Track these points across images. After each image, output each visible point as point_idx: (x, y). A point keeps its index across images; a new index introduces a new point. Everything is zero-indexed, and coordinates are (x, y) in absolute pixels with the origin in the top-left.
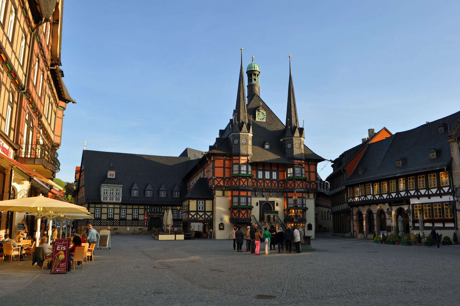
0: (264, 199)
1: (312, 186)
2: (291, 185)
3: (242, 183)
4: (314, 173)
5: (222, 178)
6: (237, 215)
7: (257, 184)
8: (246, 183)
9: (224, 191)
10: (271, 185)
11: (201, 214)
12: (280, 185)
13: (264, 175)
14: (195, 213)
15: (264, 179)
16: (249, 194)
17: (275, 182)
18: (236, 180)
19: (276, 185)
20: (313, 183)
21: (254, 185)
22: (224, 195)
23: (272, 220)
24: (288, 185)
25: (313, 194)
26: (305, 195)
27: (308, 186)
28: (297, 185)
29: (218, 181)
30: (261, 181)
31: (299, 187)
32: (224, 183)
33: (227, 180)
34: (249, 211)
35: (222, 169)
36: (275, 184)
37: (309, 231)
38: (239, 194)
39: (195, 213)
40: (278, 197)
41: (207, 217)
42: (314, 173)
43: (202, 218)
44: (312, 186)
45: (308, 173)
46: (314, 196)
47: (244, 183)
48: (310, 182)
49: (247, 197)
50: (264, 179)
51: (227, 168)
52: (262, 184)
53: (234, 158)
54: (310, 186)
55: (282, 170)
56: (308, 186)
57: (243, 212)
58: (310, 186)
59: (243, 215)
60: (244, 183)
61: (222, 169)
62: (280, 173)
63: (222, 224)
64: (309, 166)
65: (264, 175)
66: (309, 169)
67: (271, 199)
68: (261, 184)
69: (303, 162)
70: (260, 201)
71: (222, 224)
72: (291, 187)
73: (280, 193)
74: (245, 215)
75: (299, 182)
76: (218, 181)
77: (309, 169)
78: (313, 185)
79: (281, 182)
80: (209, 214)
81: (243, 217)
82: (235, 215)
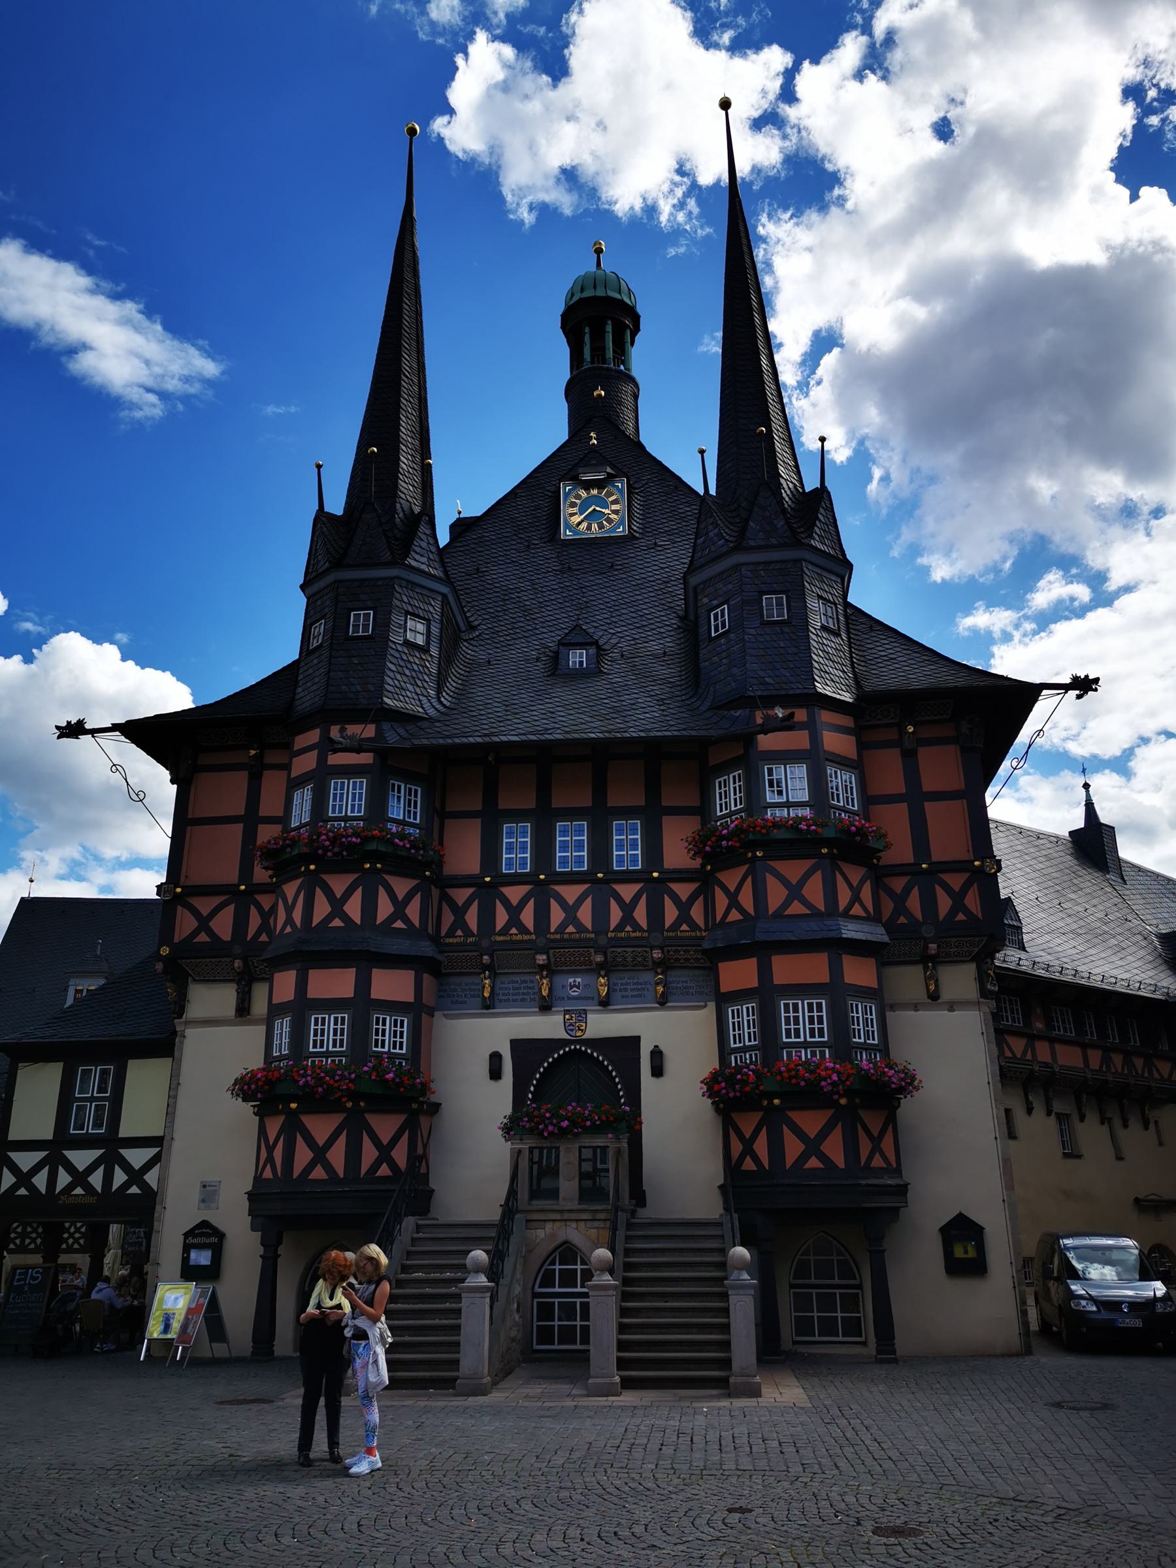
0: (548, 1026)
1: (944, 903)
2: (734, 903)
3: (322, 908)
4: (958, 808)
5: (227, 891)
7: (487, 916)
8: (353, 908)
9: (245, 983)
10: (600, 913)
11: (81, 1158)
12: (671, 913)
13: (543, 849)
14: (40, 1155)
15: (543, 880)
16: (392, 985)
17: (627, 891)
18: (290, 889)
19: (640, 914)
20: (956, 881)
21: (460, 922)
22: (243, 1010)
23: (568, 1186)
24: (721, 901)
25: (972, 967)
26: (909, 980)
27: (914, 903)
28: (776, 895)
29: (196, 913)
30: (514, 893)
31: (797, 908)
32: (240, 922)
33: (266, 901)
34: (385, 1126)
35: (239, 828)
36: (628, 909)
37: (964, 1287)
38: (302, 984)
39: (40, 1155)
40: (662, 1002)
41: (120, 1177)
42: (958, 808)
43: (89, 1188)
44: (944, 903)
45: (903, 807)
46: (982, 978)
47: (337, 905)
48: (926, 873)
49: (362, 1008)
50: (543, 880)
52: (528, 916)
53: (301, 741)
54: (929, 903)
55: (693, 801)
56: (914, 903)
57: (321, 1127)
58: (929, 903)
59: (320, 1154)
60: (337, 905)
61: (239, 828)
62: (666, 820)
63: (205, 1234)
64: (909, 756)
65: (543, 849)
66: (912, 775)
67: (603, 1024)
68: (514, 912)
69: (826, 716)
70: (516, 1044)
71: (205, 1234)
72: (735, 916)
73: (679, 978)
74: (337, 1156)
75: (793, 869)
76: (196, 913)
77: (912, 775)
79: (684, 890)
80: (137, 1157)
81: (319, 1173)
82: (271, 1149)
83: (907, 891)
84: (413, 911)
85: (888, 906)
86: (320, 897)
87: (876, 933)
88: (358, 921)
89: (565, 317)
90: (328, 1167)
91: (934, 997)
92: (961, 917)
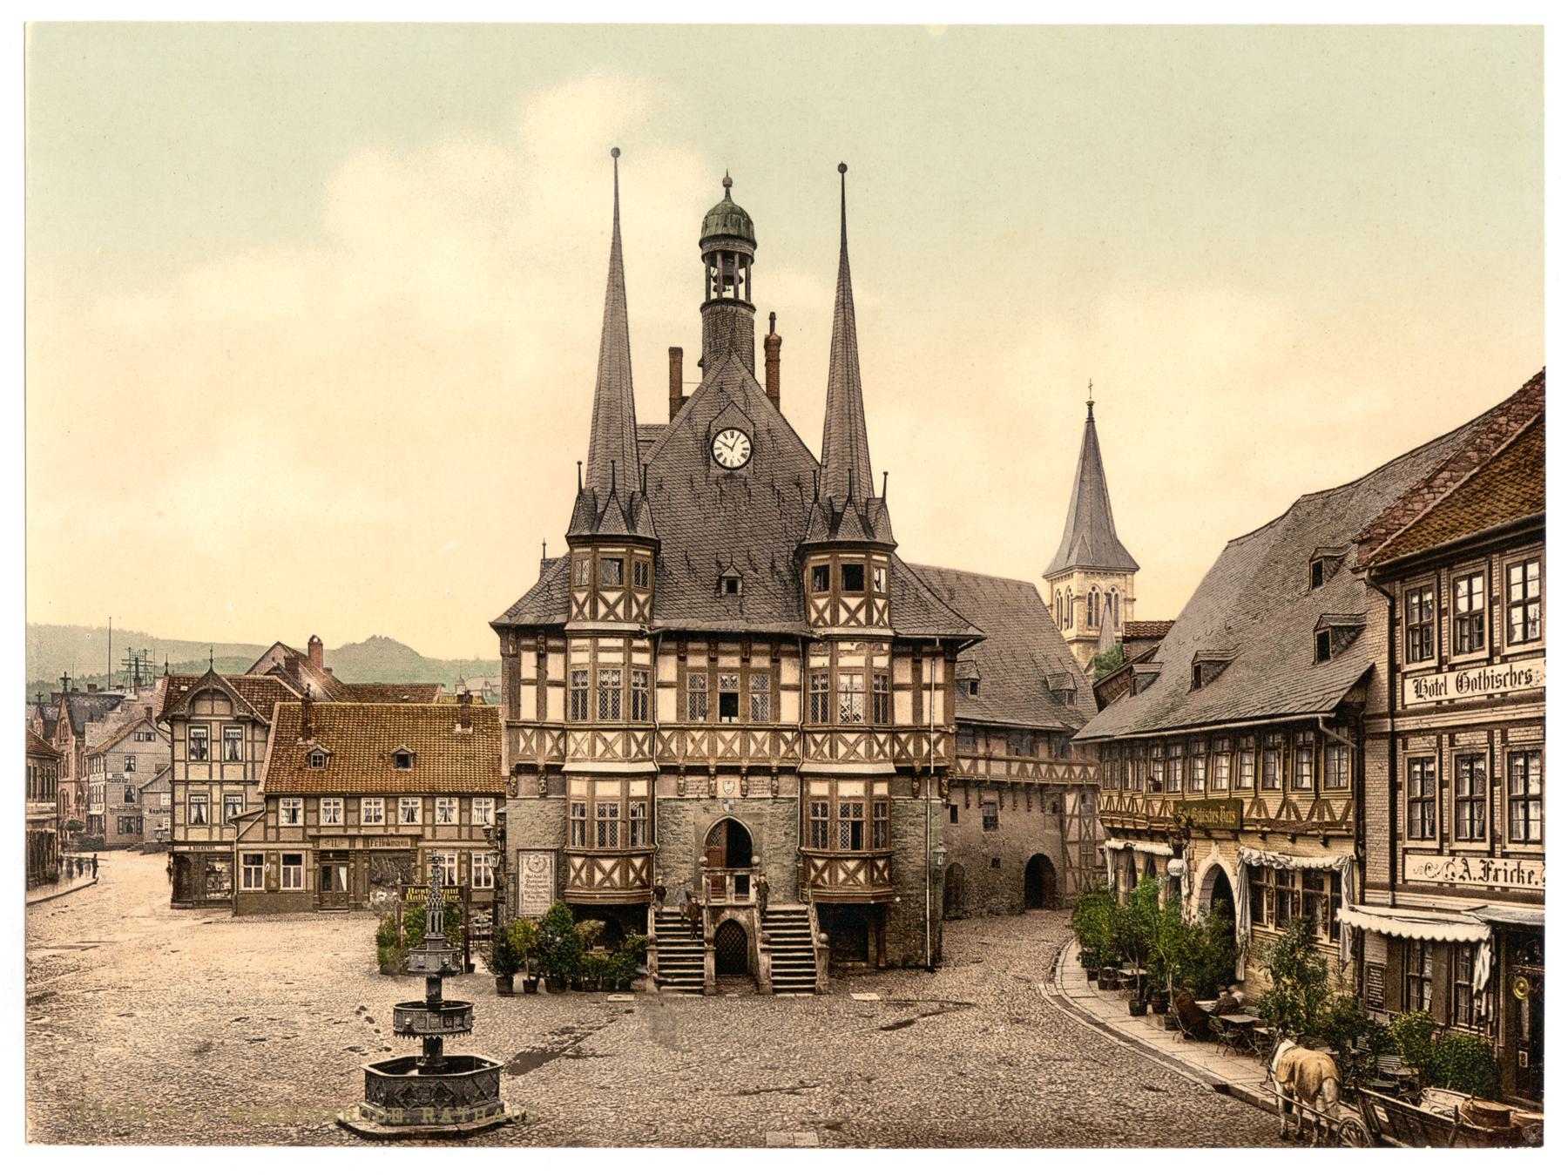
53: (575, 643)
58: (918, 748)
66: (917, 671)
83: (908, 740)
87: (890, 768)
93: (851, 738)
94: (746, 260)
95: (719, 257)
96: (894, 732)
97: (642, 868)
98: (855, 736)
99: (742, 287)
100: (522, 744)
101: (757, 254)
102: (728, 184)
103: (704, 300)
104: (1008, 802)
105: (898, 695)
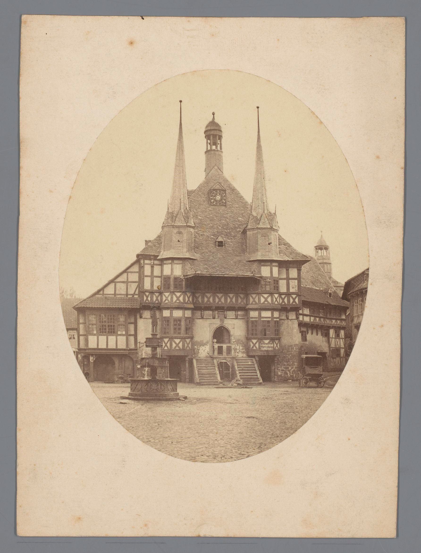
1: (291, 300)
6: (168, 345)
20: (294, 296)
24: (251, 300)
44: (291, 300)
51: (156, 277)
54: (289, 301)
56: (286, 300)
58: (289, 301)
64: (287, 270)
66: (288, 274)
78: (294, 299)
83: (285, 297)
84: (191, 299)
85: (281, 301)
86: (174, 296)
88: (182, 301)
89: (205, 132)
90: (179, 347)
91: (288, 318)
92: (294, 303)
93: (266, 296)
94: (220, 137)
95: (211, 137)
96: (280, 294)
97: (189, 343)
98: (268, 295)
99: (219, 146)
100: (145, 298)
101: (223, 135)
102: (213, 114)
103: (205, 150)
104: (310, 332)
105: (281, 281)
